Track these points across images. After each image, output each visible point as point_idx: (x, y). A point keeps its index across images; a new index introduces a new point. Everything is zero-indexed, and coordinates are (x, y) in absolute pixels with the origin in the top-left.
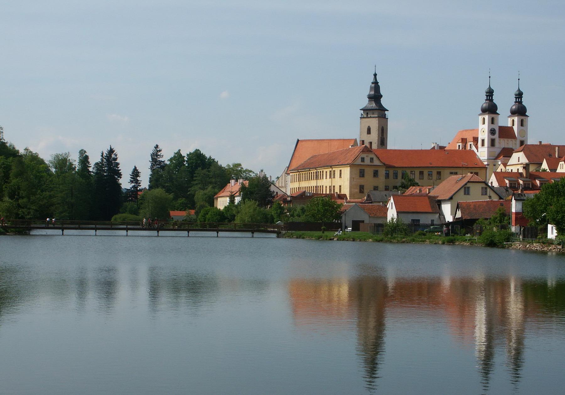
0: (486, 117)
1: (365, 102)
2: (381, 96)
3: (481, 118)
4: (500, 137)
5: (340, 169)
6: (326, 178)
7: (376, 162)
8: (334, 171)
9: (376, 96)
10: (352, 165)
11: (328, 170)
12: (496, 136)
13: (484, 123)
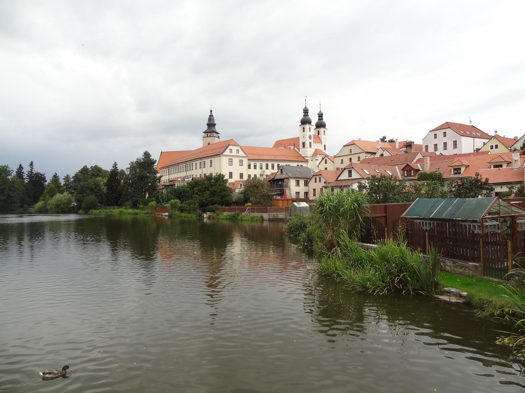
1: (206, 128)
5: (211, 159)
6: (196, 169)
7: (241, 153)
8: (204, 162)
11: (198, 162)
12: (312, 141)
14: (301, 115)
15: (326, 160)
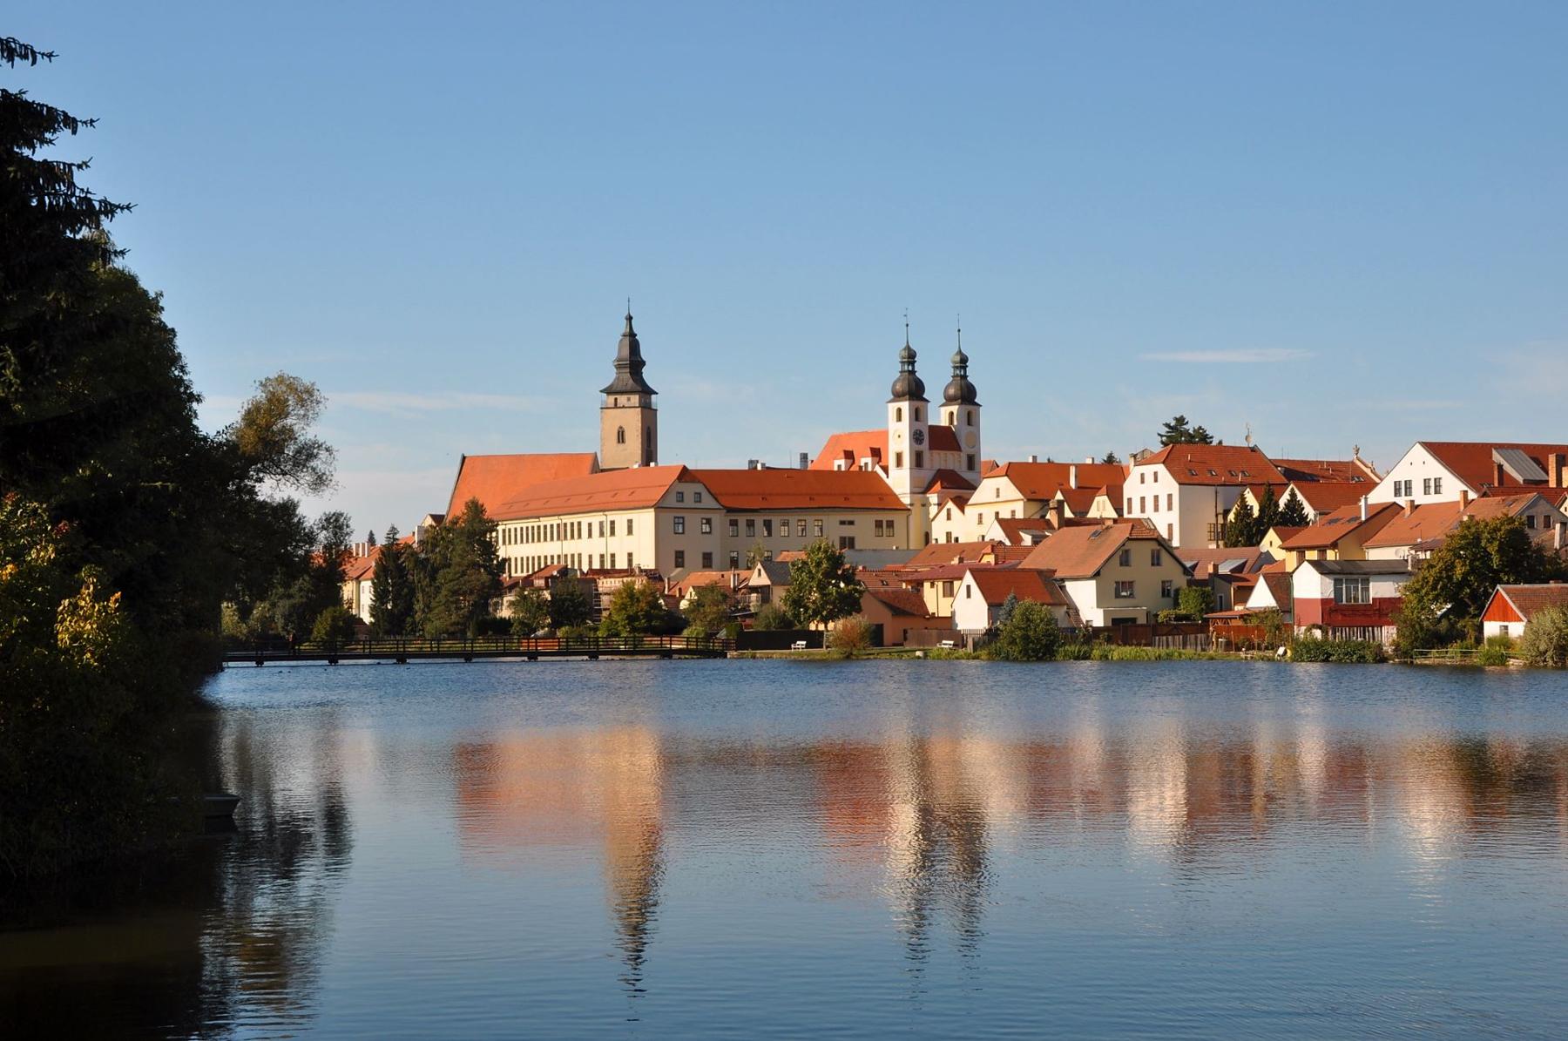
0: (905, 405)
1: (610, 376)
2: (643, 363)
3: (893, 407)
4: (931, 448)
8: (613, 523)
10: (659, 508)
11: (595, 519)
13: (899, 419)
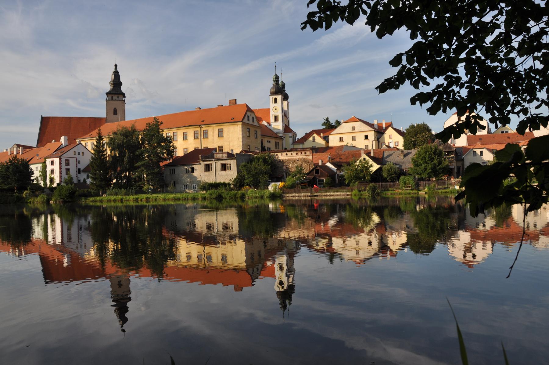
0: (279, 97)
9: (117, 82)
10: (244, 124)
11: (190, 132)
14: (271, 84)
15: (314, 137)
